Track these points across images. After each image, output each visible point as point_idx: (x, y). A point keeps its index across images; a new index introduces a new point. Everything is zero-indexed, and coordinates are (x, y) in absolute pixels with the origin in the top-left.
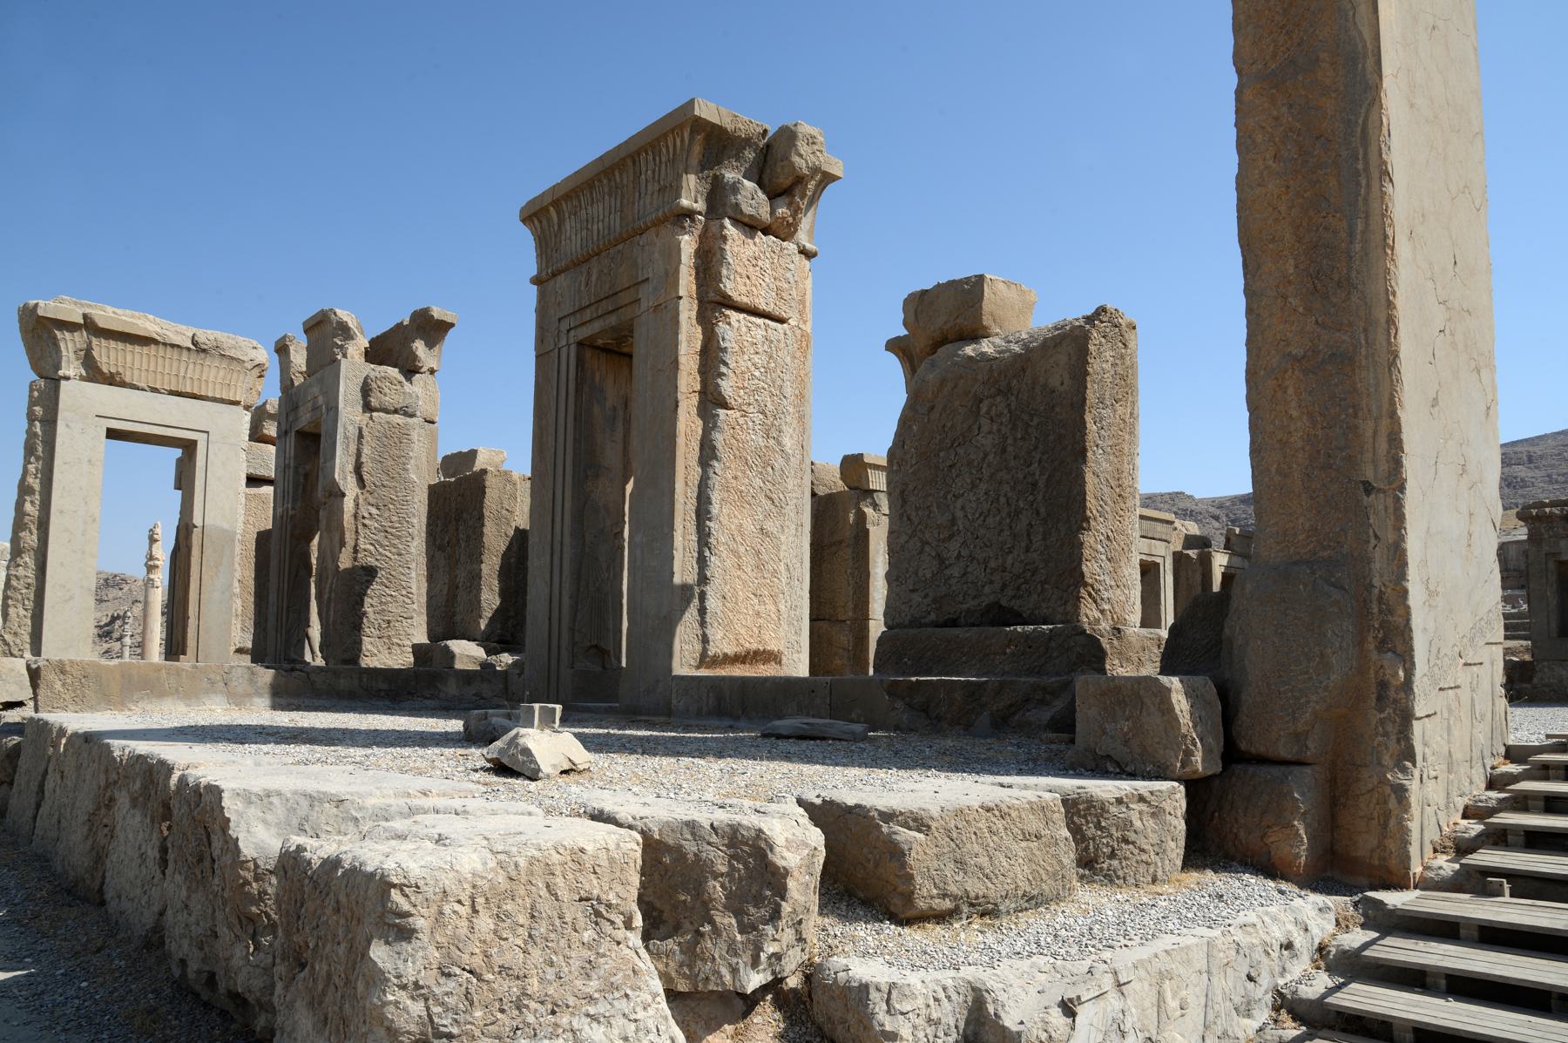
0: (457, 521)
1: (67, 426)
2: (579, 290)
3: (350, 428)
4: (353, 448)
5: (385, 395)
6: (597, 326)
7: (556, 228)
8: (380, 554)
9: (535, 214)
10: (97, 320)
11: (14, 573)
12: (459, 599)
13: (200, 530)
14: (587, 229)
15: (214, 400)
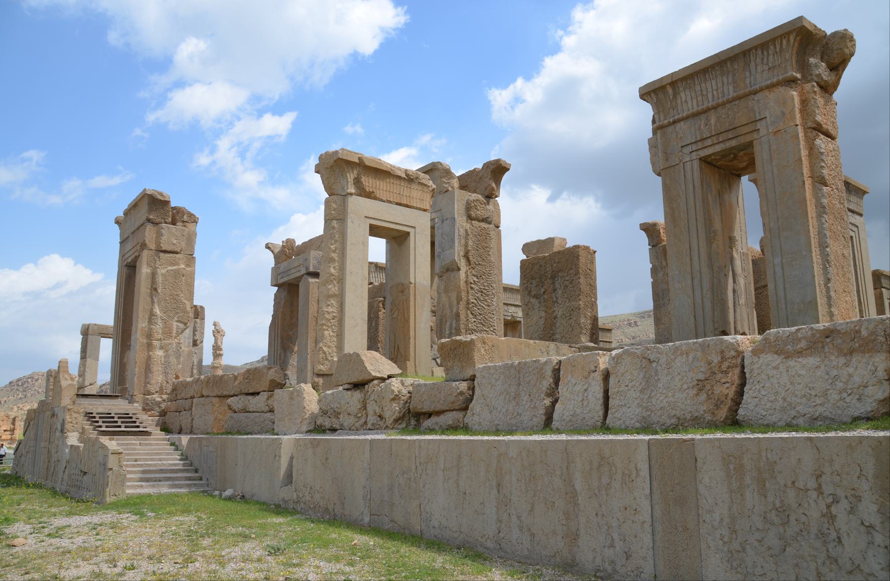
0: (553, 277)
1: (352, 222)
2: (699, 129)
3: (461, 230)
4: (463, 241)
5: (478, 210)
6: (718, 148)
7: (671, 97)
8: (480, 305)
9: (655, 91)
10: (365, 161)
11: (326, 310)
12: (558, 324)
13: (413, 285)
14: (702, 95)
15: (417, 208)
